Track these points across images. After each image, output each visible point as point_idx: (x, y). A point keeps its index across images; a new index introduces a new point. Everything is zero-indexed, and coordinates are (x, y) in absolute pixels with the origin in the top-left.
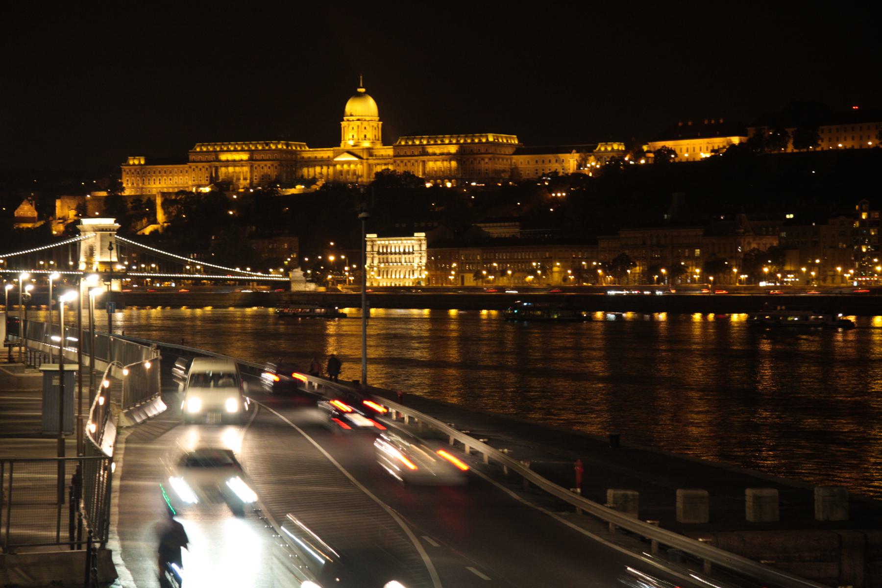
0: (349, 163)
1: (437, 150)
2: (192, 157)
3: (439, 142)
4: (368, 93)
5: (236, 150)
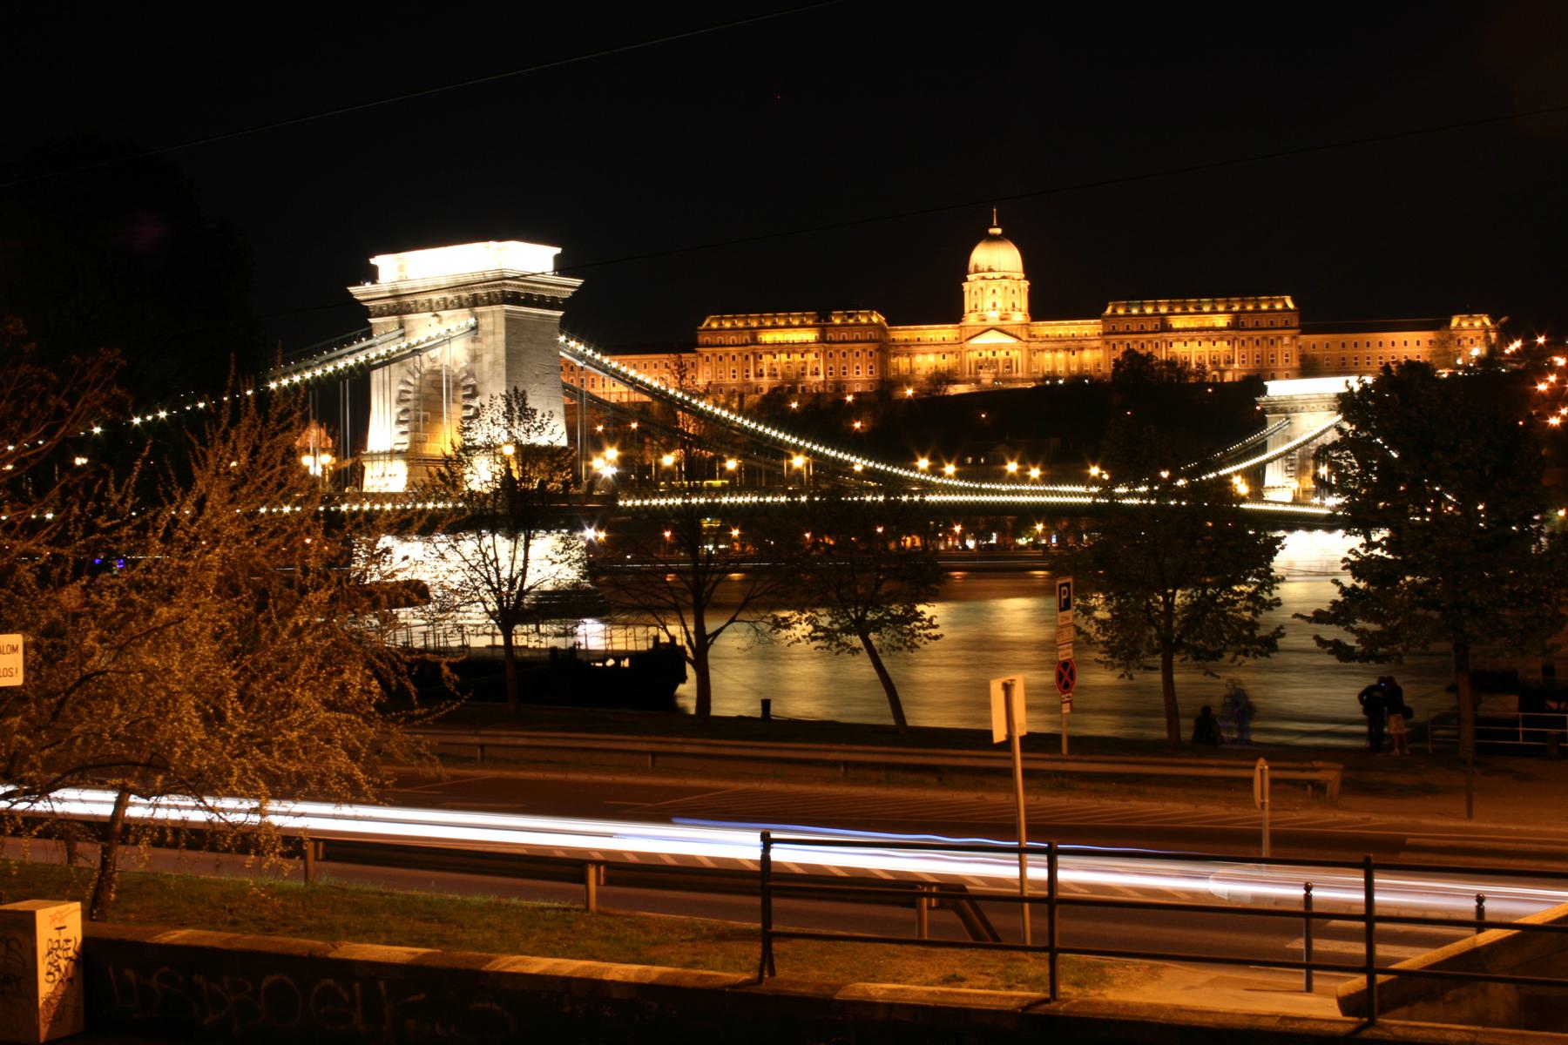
0: (1000, 347)
1: (1191, 322)
2: (702, 339)
3: (1191, 310)
4: (1009, 236)
5: (789, 326)
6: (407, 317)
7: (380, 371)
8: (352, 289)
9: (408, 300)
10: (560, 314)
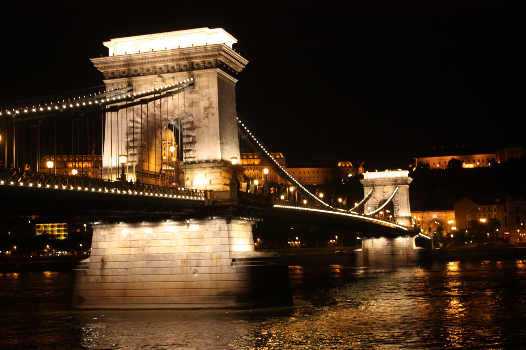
3: (245, 157)
6: (135, 79)
7: (139, 106)
8: (94, 60)
9: (133, 68)
10: (236, 81)
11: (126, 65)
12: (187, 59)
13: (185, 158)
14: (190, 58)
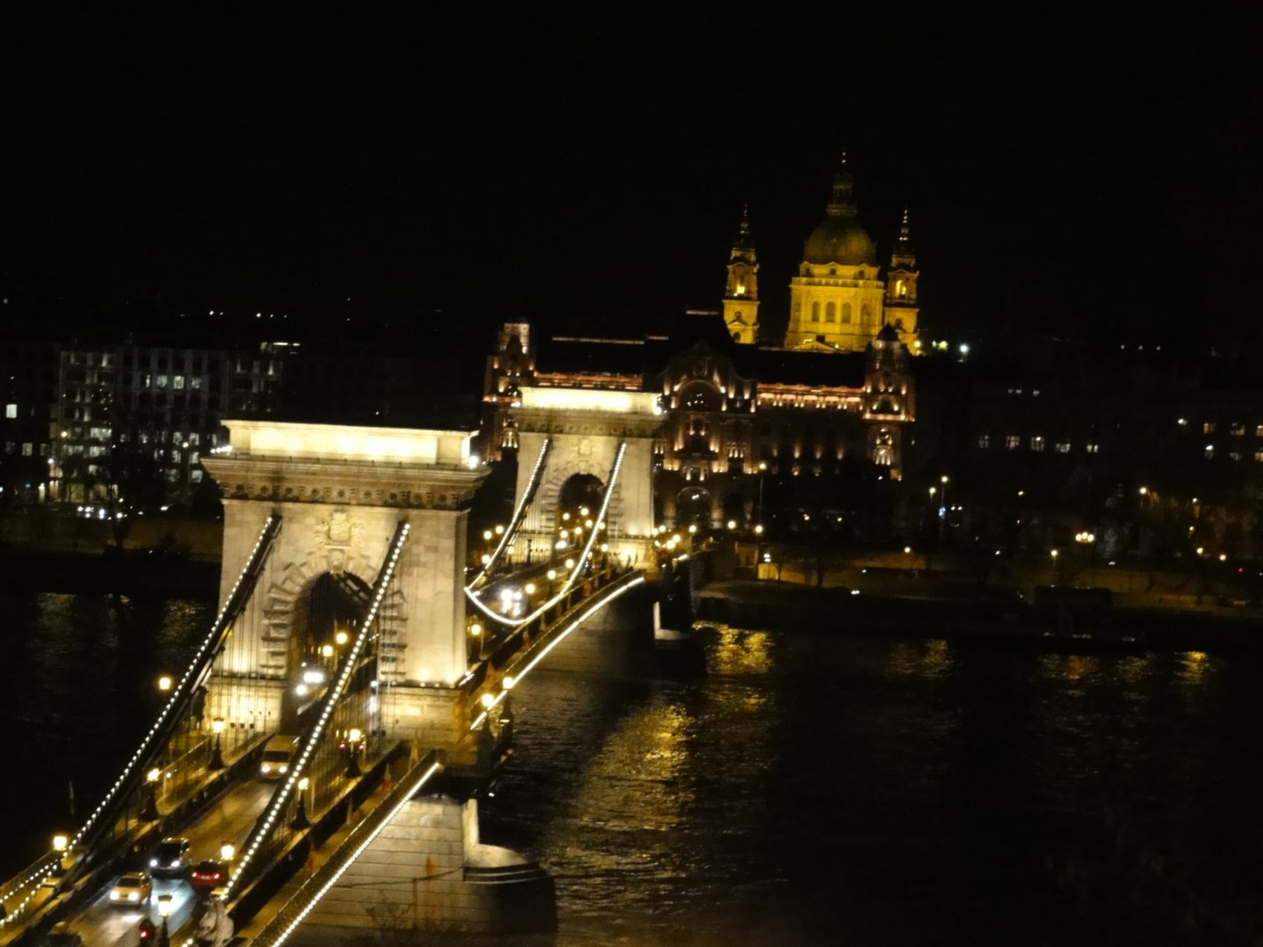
9: (289, 485)
11: (272, 479)
12: (400, 485)
13: (383, 673)
14: (407, 485)
